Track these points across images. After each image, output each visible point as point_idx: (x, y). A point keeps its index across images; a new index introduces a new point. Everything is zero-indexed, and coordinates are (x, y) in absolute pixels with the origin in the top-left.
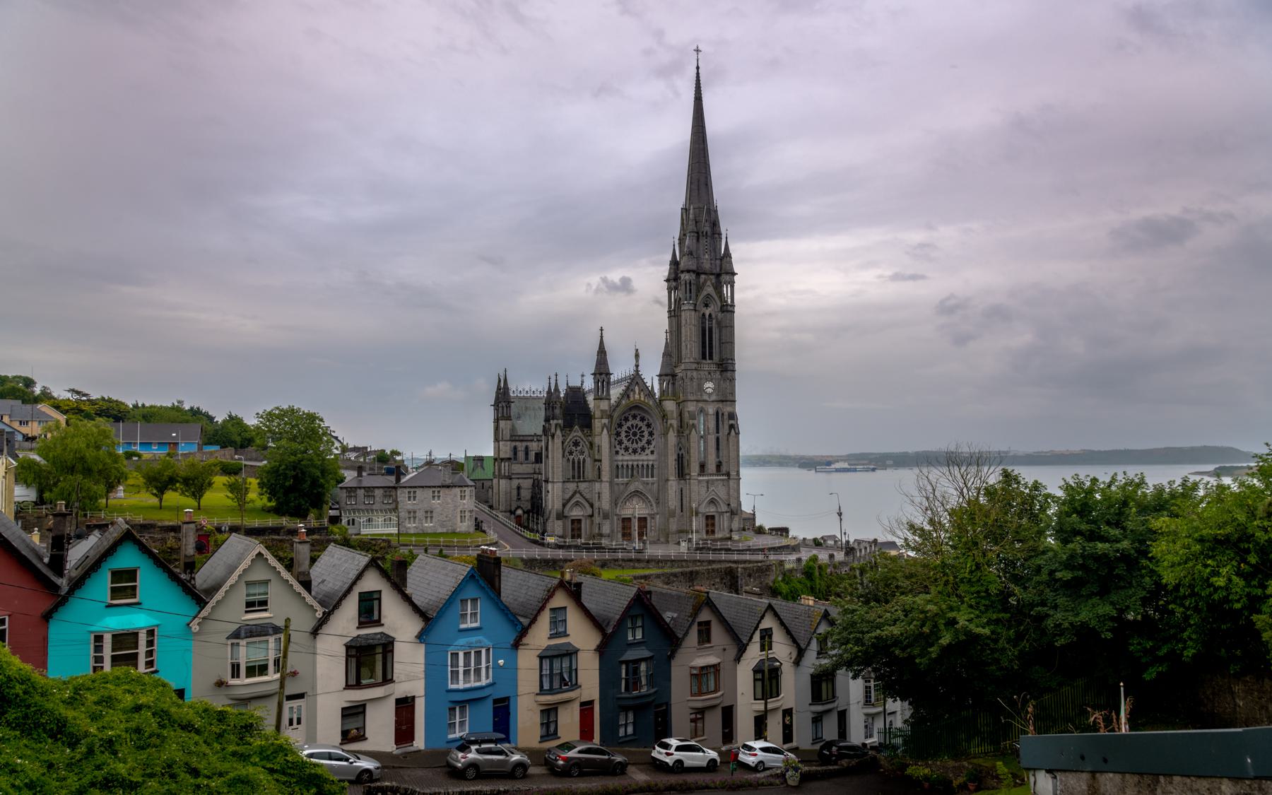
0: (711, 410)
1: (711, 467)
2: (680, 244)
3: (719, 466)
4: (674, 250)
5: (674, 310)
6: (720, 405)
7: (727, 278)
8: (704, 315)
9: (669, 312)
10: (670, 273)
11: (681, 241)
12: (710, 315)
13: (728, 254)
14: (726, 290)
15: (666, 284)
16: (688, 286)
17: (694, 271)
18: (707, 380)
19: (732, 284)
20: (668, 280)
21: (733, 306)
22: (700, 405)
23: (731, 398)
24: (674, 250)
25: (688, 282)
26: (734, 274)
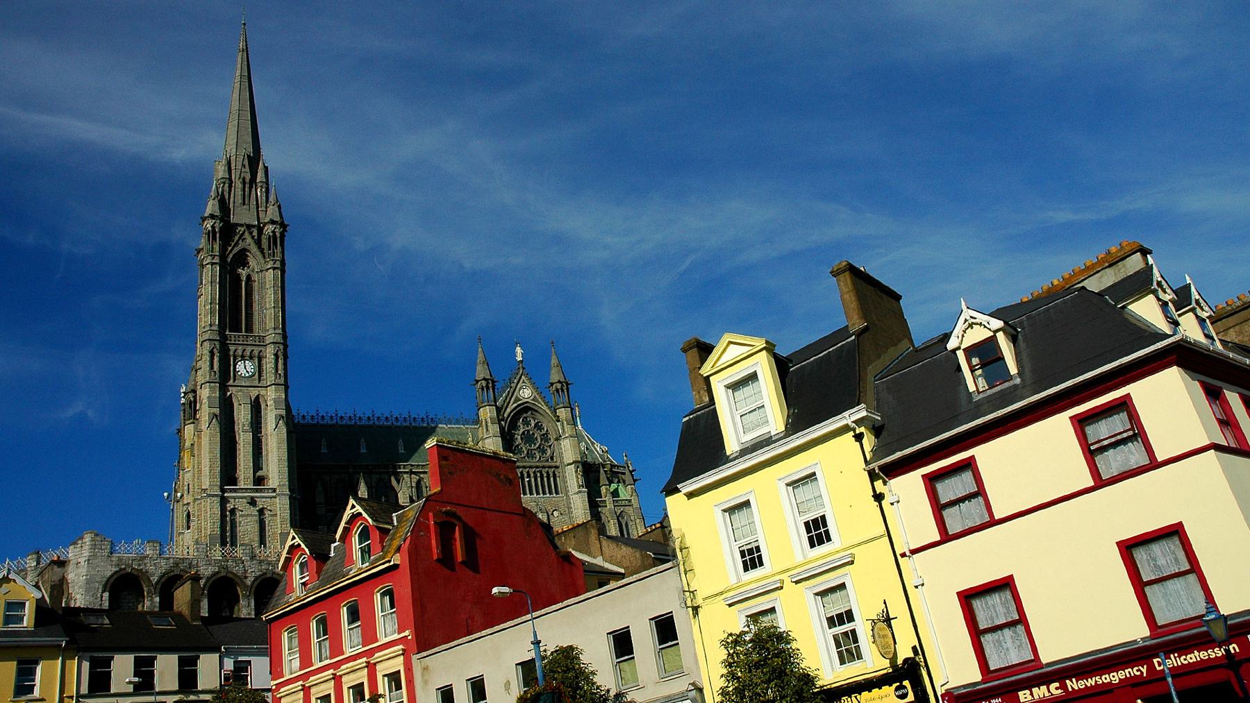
3: (259, 481)
6: (263, 392)
8: (238, 277)
12: (249, 277)
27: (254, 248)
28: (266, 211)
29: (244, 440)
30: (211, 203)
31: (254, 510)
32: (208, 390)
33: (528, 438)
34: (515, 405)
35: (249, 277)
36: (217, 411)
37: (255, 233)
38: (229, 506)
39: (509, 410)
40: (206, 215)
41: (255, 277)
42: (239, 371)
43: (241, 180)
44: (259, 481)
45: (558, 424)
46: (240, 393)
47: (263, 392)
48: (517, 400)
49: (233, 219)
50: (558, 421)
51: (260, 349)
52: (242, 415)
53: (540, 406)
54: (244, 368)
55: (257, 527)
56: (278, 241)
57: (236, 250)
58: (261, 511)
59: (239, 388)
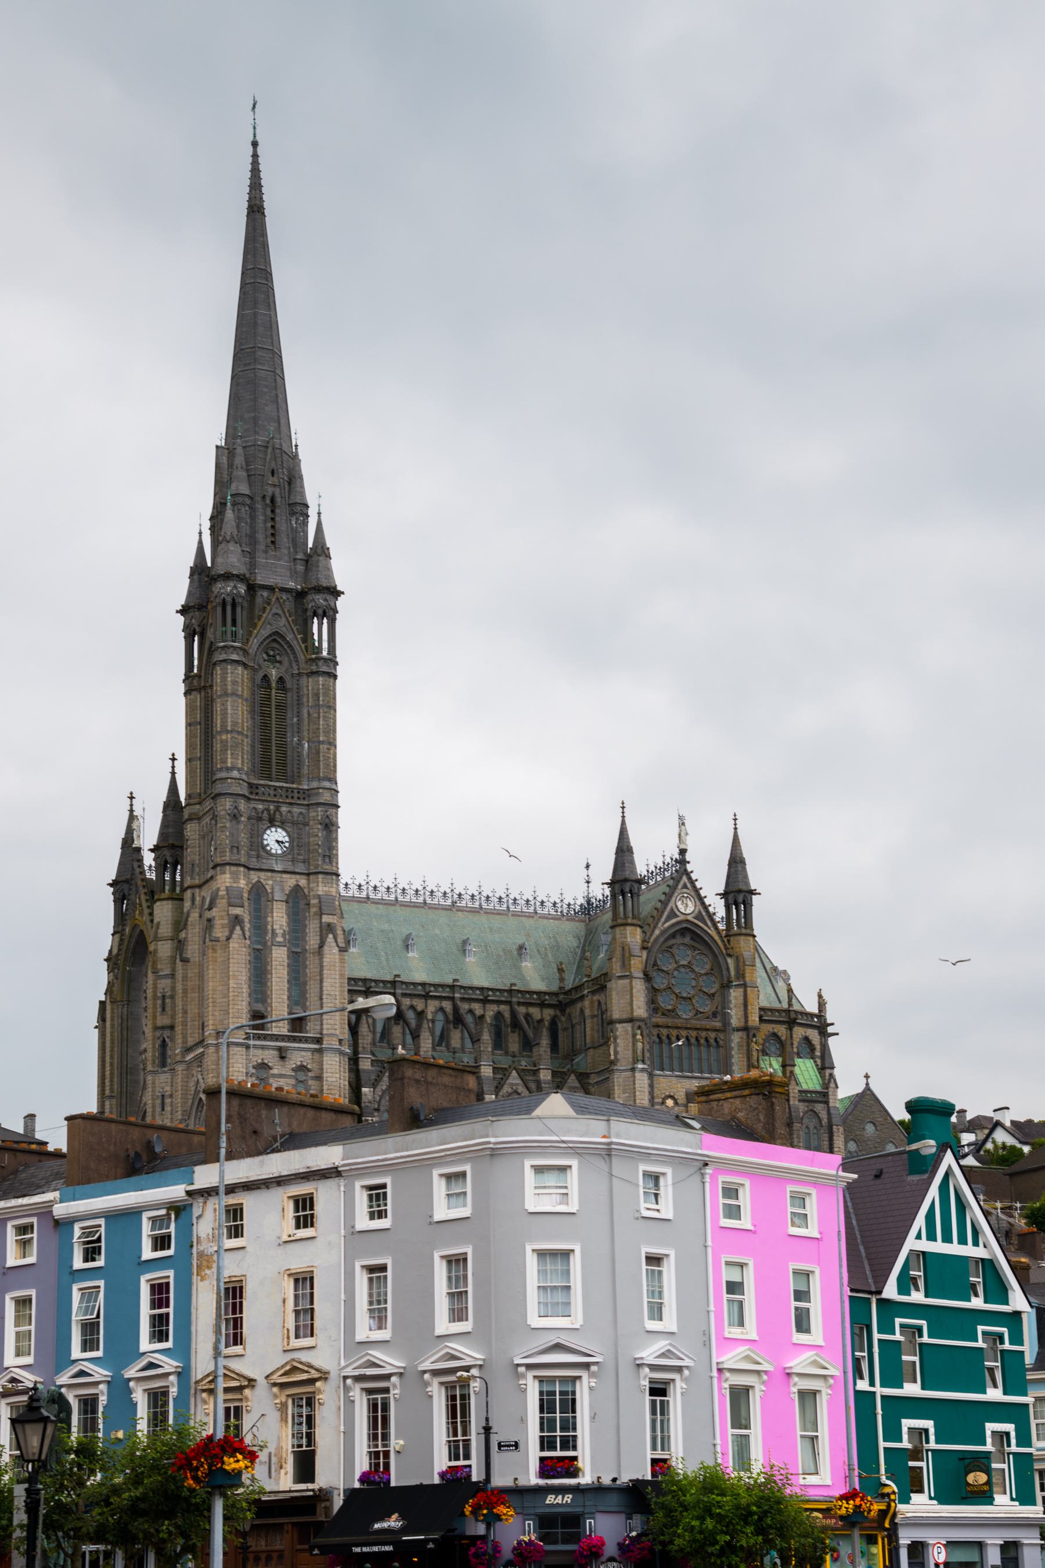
0: (280, 885)
2: (212, 529)
3: (297, 1024)
4: (200, 542)
5: (199, 676)
6: (303, 882)
7: (320, 599)
8: (266, 678)
9: (188, 678)
10: (190, 594)
11: (217, 519)
12: (281, 680)
13: (322, 550)
14: (318, 629)
15: (181, 620)
16: (229, 609)
17: (241, 578)
18: (272, 823)
19: (330, 614)
20: (184, 611)
21: (332, 661)
22: (254, 876)
23: (327, 868)
24: (200, 542)
25: (229, 599)
26: (337, 593)
28: (307, 561)
32: (228, 876)
34: (667, 925)
39: (657, 932)
42: (268, 845)
43: (268, 501)
45: (730, 961)
46: (270, 882)
47: (303, 882)
48: (673, 914)
49: (261, 579)
50: (730, 956)
51: (299, 810)
53: (706, 928)
57: (265, 632)
59: (269, 874)
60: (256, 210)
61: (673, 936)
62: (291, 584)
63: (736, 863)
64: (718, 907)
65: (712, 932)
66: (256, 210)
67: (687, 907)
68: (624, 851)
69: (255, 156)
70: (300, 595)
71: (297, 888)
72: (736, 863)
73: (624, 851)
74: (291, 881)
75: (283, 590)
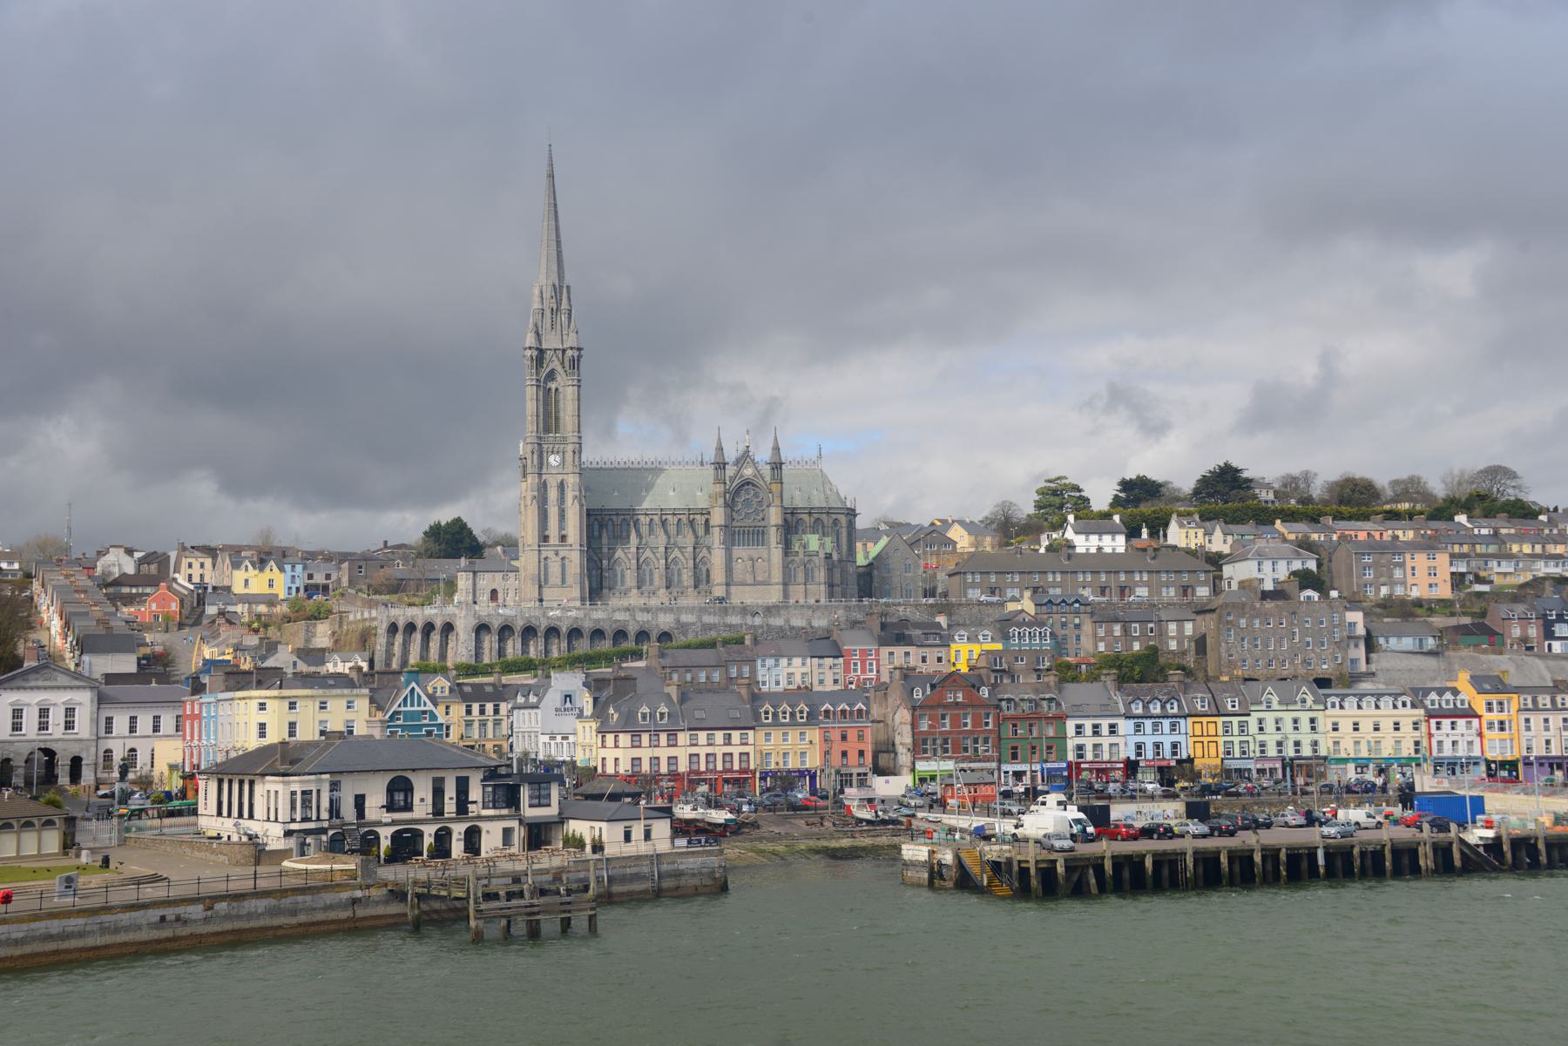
1: (554, 539)
6: (565, 477)
8: (550, 389)
12: (557, 389)
17: (537, 349)
27: (559, 368)
29: (553, 511)
30: (529, 335)
31: (559, 559)
33: (747, 503)
35: (557, 389)
36: (536, 493)
37: (560, 356)
38: (543, 556)
40: (527, 346)
41: (561, 389)
44: (563, 538)
48: (742, 476)
49: (544, 346)
52: (553, 494)
54: (554, 460)
55: (560, 570)
56: (575, 363)
57: (548, 370)
58: (563, 559)
60: (551, 176)
61: (743, 485)
62: (561, 347)
63: (776, 449)
64: (766, 471)
65: (761, 482)
66: (551, 176)
67: (748, 472)
68: (720, 449)
69: (550, 151)
70: (564, 351)
71: (562, 482)
72: (776, 449)
73: (720, 449)
74: (560, 478)
75: (555, 350)
